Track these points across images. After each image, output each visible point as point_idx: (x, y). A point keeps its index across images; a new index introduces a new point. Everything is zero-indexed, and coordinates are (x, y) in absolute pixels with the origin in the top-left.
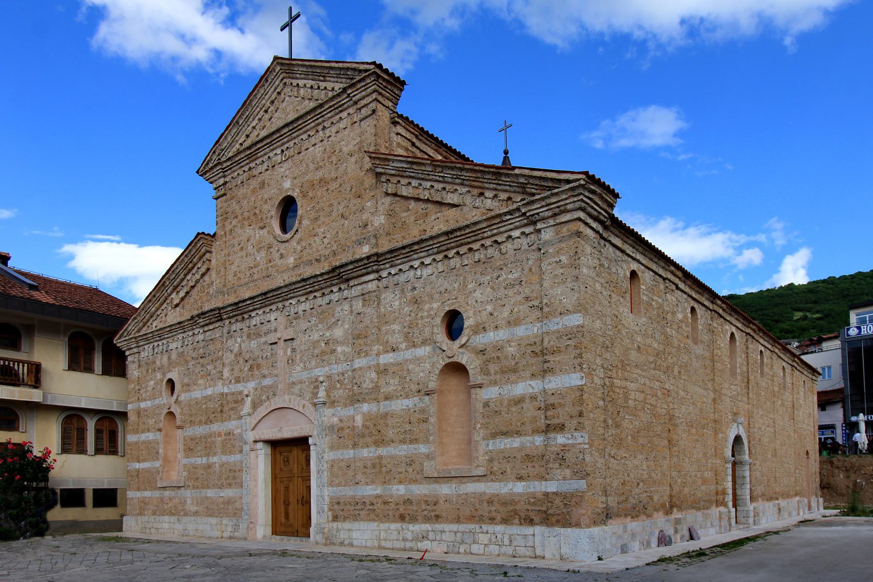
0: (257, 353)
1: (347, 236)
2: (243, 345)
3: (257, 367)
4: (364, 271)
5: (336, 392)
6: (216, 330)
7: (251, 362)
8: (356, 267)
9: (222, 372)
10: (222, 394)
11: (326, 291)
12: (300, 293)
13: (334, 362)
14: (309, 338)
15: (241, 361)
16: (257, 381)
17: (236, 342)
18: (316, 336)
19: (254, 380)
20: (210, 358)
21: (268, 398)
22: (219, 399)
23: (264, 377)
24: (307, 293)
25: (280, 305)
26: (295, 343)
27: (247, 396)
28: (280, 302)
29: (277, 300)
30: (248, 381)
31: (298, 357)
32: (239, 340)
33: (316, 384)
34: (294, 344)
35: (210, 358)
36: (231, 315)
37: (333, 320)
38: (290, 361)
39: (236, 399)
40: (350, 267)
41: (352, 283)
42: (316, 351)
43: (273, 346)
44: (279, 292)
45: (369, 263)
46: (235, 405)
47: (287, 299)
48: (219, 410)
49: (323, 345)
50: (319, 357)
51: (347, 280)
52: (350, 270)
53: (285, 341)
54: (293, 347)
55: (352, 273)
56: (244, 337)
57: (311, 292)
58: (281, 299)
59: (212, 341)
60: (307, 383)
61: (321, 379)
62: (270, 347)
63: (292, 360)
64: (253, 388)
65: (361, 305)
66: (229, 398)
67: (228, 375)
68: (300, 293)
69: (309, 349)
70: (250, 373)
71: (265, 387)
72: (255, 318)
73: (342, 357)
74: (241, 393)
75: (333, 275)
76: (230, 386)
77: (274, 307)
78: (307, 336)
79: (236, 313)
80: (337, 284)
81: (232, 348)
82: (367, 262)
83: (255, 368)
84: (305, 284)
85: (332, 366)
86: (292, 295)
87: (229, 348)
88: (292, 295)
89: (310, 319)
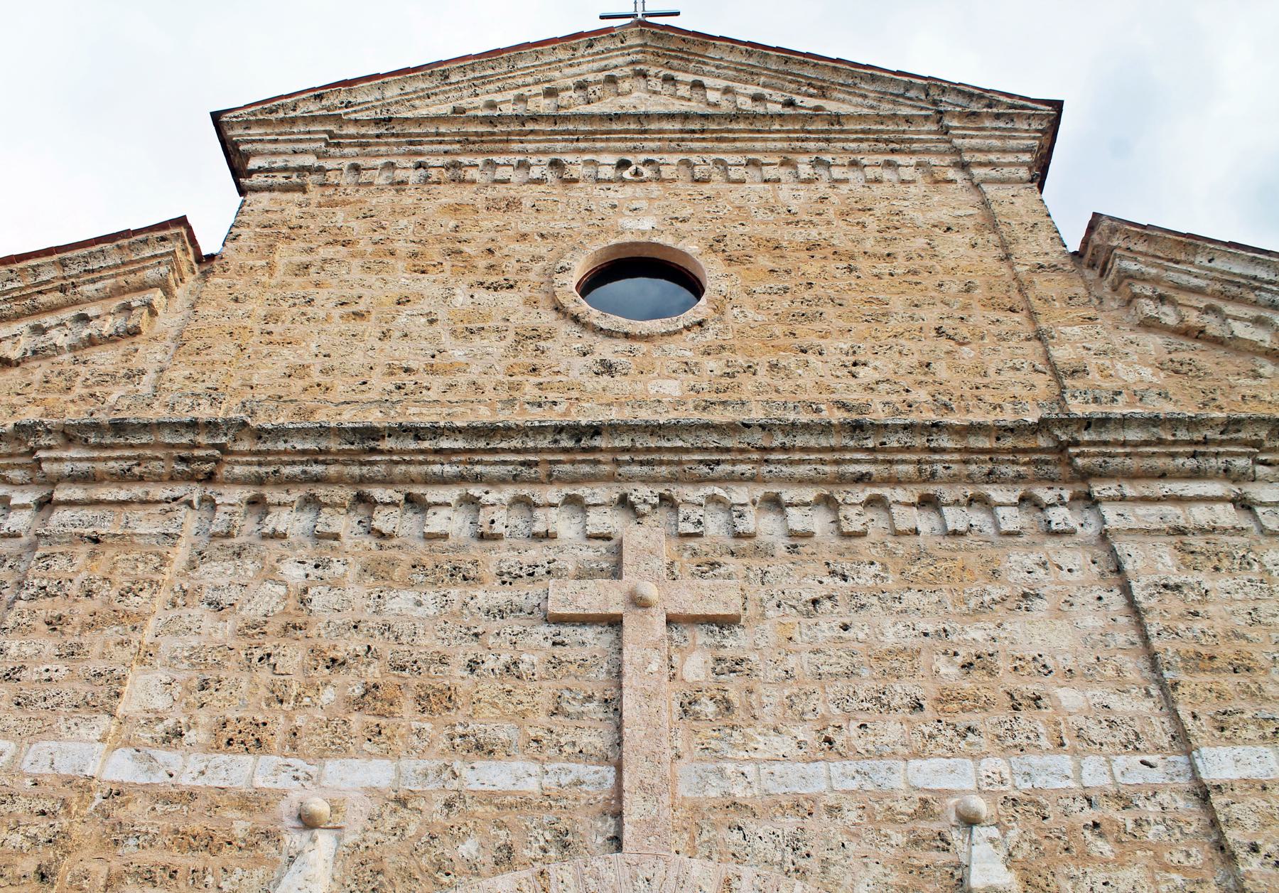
0: (428, 643)
1: (979, 380)
2: (319, 597)
3: (418, 699)
4: (1191, 463)
5: (1101, 877)
6: (140, 512)
7: (374, 673)
8: (1160, 442)
9: (121, 680)
10: (84, 786)
11: (948, 493)
12: (802, 470)
13: (1044, 742)
14: (845, 634)
15: (292, 656)
16: (410, 765)
17: (270, 574)
18: (892, 634)
19: (386, 754)
20: (47, 608)
21: (506, 857)
22: (48, 805)
23: (483, 749)
24: (841, 480)
25: (642, 493)
26: (735, 643)
27: (308, 822)
28: (646, 480)
29: (636, 469)
30: (337, 747)
31: (771, 697)
32: (293, 573)
33: (927, 827)
34: (729, 642)
35: (47, 608)
36: (287, 470)
37: (996, 592)
38: (709, 708)
39: (197, 826)
40: (1133, 435)
41: (1100, 489)
42: (902, 690)
43: (566, 630)
44: (680, 444)
45: (1221, 443)
46: (185, 861)
47: (700, 481)
48: (28, 865)
49: (949, 670)
50: (929, 713)
51: (1086, 475)
52: (1124, 444)
53: (671, 621)
54: (722, 653)
55: (1127, 455)
56: (338, 568)
57: (862, 479)
58: (664, 470)
59: (86, 548)
60: (852, 816)
61: (980, 805)
62: (545, 629)
63: (727, 706)
64: (371, 792)
65: (1168, 559)
66: (137, 812)
67: (161, 702)
68: (802, 470)
69: (849, 675)
70: (356, 719)
71: (489, 797)
72: (444, 512)
73: (1096, 732)
74: (248, 802)
75: (1022, 445)
76: (162, 755)
77: (602, 493)
78: (826, 625)
79: (333, 470)
80: (1019, 478)
81: (225, 598)
82: (1218, 437)
83: (407, 708)
84: (852, 443)
85: (1035, 760)
86: (740, 468)
87: (207, 593)
88: (740, 468)
89: (844, 565)
